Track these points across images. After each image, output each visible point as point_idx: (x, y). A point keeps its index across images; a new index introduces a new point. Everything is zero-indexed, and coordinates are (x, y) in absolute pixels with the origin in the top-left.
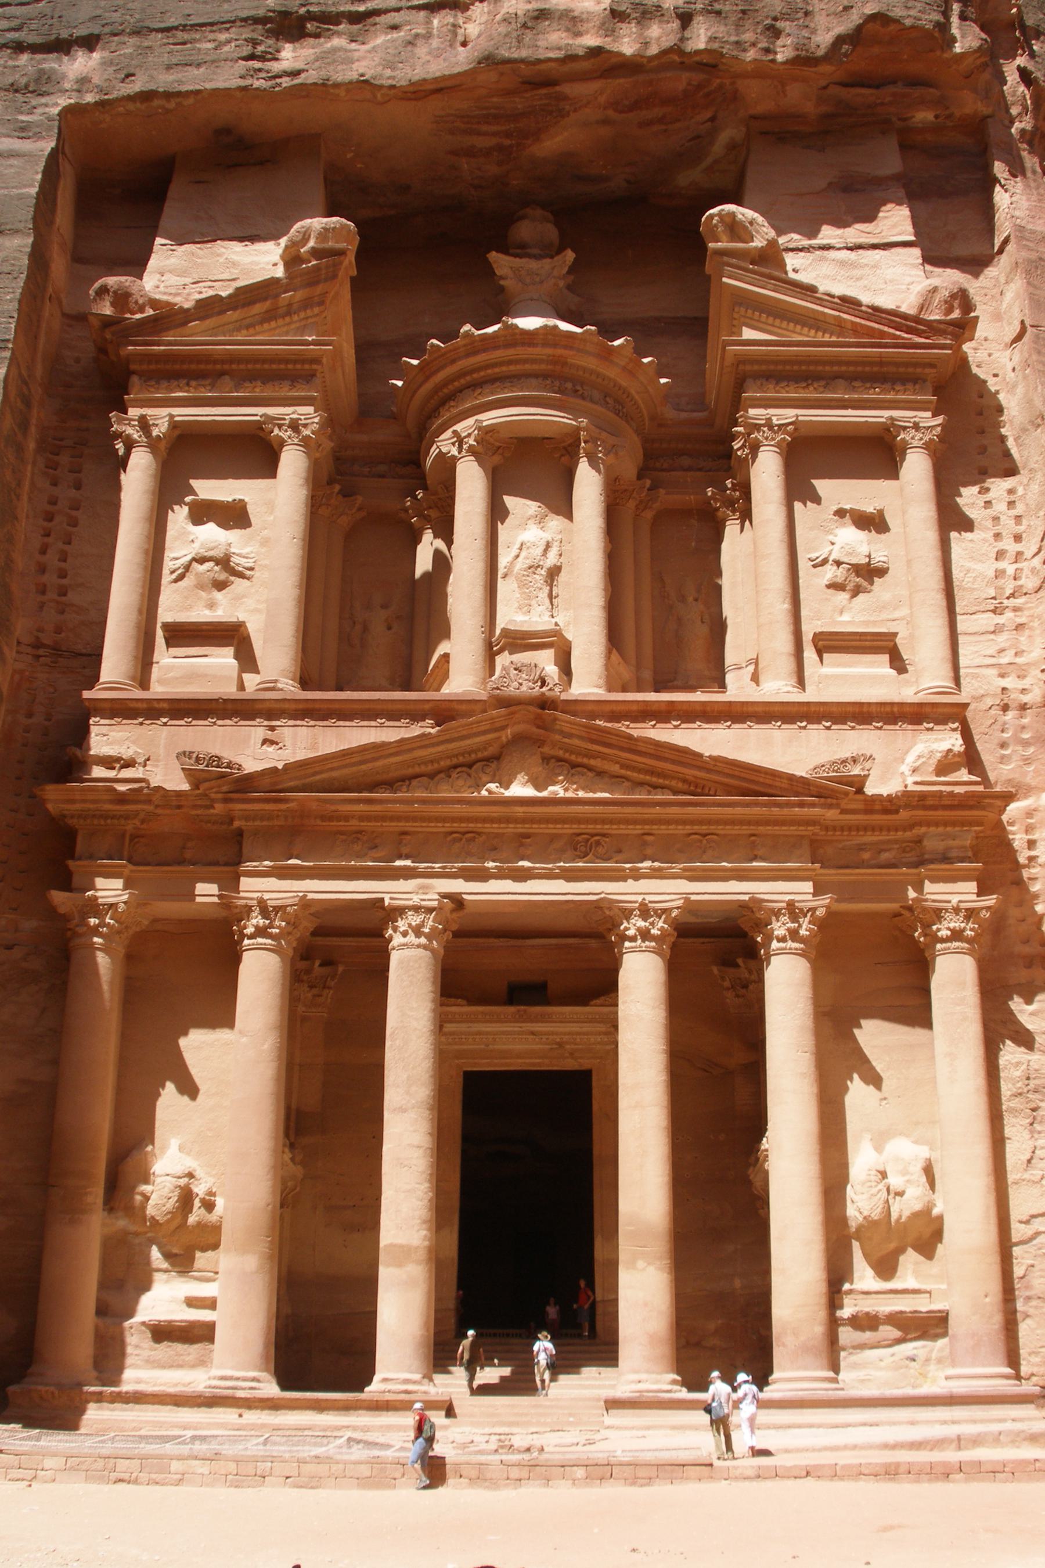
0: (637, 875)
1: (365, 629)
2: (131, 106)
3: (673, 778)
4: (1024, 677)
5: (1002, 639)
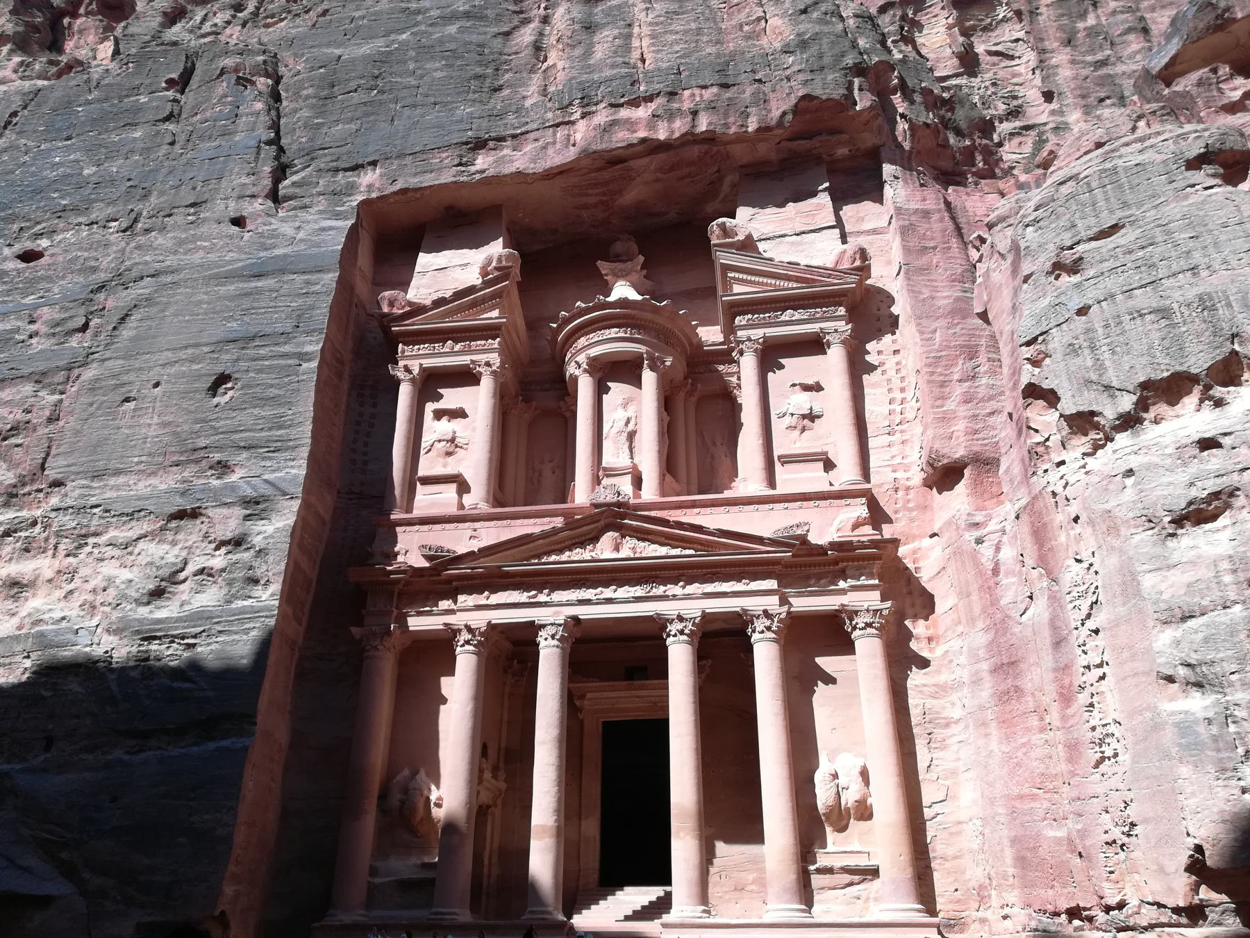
1: (540, 475)
2: (397, 198)
5: (894, 450)
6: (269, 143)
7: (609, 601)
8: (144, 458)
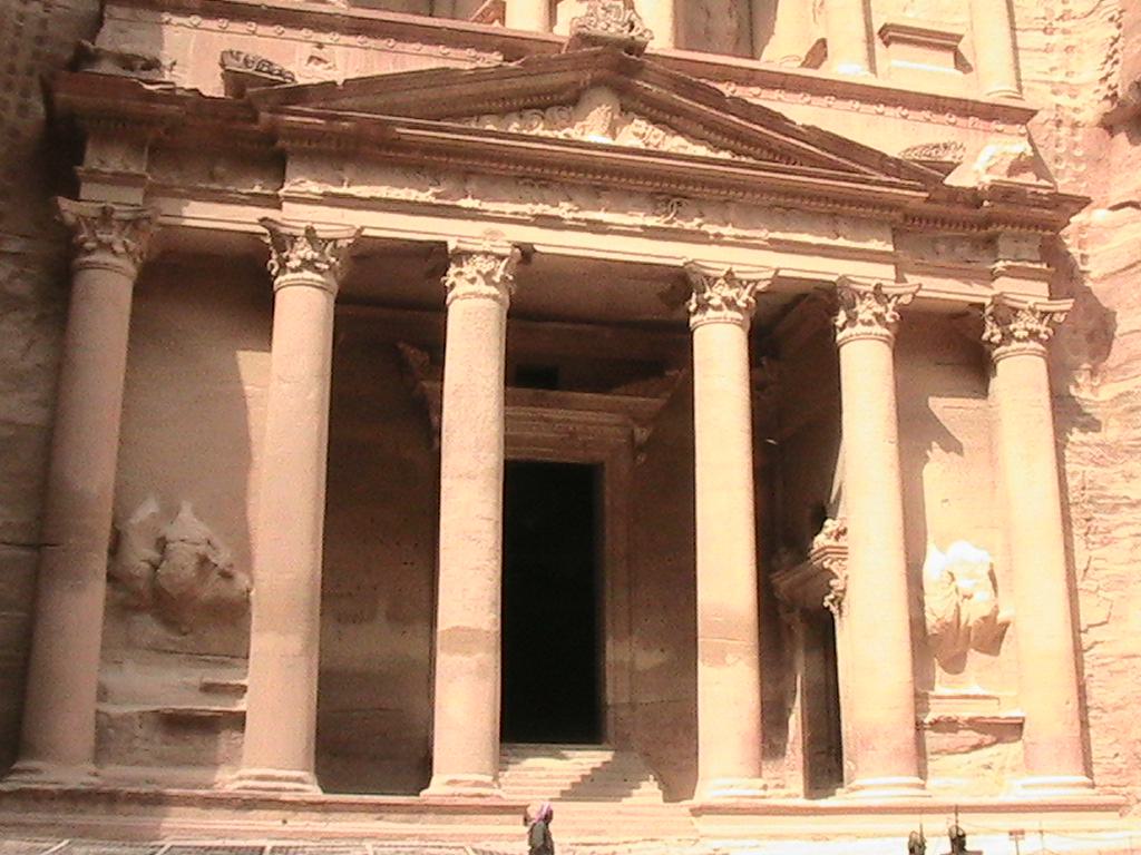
0: (718, 240)
3: (757, 146)
4: (1074, 97)
5: (1054, 59)
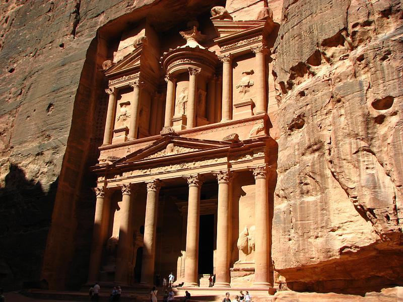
2: (110, 24)
6: (73, 13)
7: (169, 172)
8: (31, 136)
